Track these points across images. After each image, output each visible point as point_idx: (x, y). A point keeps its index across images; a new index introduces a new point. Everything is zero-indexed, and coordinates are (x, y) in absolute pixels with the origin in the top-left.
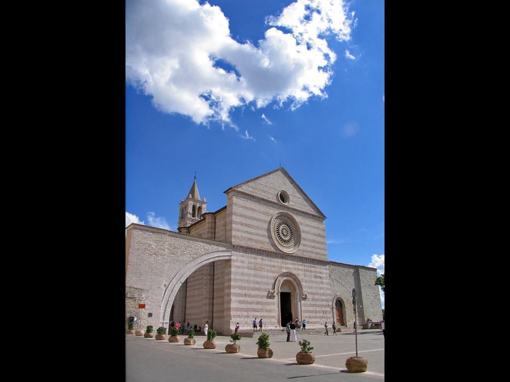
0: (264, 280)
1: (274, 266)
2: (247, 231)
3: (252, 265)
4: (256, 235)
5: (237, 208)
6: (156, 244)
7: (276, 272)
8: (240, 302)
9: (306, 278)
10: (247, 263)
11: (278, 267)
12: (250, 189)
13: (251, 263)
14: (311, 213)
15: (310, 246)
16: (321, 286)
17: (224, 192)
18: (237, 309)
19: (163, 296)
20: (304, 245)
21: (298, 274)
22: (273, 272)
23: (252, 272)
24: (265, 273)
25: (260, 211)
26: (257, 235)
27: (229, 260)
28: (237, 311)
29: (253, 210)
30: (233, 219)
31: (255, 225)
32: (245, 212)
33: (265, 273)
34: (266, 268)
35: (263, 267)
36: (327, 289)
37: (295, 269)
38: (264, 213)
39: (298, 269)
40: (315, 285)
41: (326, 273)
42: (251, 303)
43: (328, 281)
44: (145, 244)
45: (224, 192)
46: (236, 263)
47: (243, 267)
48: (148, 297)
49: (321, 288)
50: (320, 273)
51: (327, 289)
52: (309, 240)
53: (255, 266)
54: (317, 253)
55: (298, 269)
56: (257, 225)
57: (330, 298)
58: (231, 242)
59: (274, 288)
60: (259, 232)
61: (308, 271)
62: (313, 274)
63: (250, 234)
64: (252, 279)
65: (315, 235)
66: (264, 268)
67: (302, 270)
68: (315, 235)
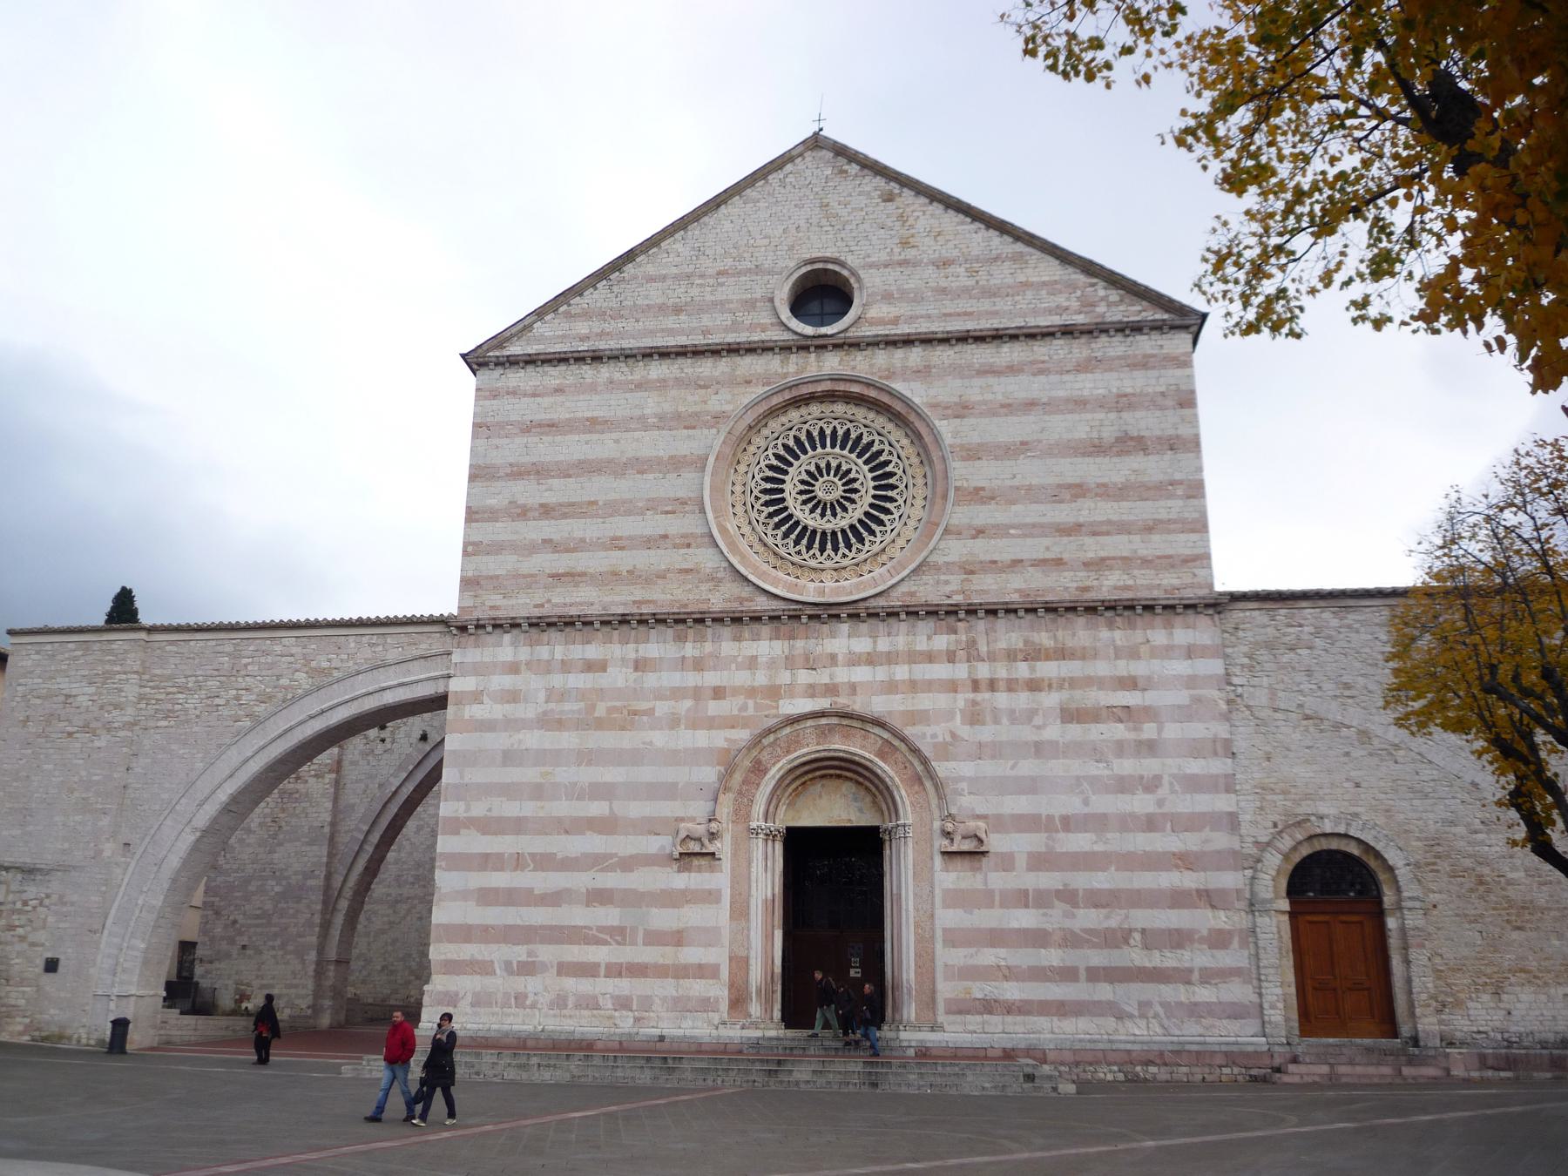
1: (718, 693)
2: (544, 541)
9: (986, 733)
11: (752, 692)
12: (582, 328)
14: (1057, 320)
20: (979, 532)
21: (916, 717)
22: (712, 724)
25: (642, 418)
26: (616, 544)
29: (594, 425)
31: (601, 499)
32: (545, 449)
37: (891, 687)
38: (667, 422)
39: (914, 686)
40: (1057, 767)
55: (914, 686)
56: (613, 496)
57: (1221, 841)
61: (1011, 686)
63: (574, 550)
67: (952, 687)
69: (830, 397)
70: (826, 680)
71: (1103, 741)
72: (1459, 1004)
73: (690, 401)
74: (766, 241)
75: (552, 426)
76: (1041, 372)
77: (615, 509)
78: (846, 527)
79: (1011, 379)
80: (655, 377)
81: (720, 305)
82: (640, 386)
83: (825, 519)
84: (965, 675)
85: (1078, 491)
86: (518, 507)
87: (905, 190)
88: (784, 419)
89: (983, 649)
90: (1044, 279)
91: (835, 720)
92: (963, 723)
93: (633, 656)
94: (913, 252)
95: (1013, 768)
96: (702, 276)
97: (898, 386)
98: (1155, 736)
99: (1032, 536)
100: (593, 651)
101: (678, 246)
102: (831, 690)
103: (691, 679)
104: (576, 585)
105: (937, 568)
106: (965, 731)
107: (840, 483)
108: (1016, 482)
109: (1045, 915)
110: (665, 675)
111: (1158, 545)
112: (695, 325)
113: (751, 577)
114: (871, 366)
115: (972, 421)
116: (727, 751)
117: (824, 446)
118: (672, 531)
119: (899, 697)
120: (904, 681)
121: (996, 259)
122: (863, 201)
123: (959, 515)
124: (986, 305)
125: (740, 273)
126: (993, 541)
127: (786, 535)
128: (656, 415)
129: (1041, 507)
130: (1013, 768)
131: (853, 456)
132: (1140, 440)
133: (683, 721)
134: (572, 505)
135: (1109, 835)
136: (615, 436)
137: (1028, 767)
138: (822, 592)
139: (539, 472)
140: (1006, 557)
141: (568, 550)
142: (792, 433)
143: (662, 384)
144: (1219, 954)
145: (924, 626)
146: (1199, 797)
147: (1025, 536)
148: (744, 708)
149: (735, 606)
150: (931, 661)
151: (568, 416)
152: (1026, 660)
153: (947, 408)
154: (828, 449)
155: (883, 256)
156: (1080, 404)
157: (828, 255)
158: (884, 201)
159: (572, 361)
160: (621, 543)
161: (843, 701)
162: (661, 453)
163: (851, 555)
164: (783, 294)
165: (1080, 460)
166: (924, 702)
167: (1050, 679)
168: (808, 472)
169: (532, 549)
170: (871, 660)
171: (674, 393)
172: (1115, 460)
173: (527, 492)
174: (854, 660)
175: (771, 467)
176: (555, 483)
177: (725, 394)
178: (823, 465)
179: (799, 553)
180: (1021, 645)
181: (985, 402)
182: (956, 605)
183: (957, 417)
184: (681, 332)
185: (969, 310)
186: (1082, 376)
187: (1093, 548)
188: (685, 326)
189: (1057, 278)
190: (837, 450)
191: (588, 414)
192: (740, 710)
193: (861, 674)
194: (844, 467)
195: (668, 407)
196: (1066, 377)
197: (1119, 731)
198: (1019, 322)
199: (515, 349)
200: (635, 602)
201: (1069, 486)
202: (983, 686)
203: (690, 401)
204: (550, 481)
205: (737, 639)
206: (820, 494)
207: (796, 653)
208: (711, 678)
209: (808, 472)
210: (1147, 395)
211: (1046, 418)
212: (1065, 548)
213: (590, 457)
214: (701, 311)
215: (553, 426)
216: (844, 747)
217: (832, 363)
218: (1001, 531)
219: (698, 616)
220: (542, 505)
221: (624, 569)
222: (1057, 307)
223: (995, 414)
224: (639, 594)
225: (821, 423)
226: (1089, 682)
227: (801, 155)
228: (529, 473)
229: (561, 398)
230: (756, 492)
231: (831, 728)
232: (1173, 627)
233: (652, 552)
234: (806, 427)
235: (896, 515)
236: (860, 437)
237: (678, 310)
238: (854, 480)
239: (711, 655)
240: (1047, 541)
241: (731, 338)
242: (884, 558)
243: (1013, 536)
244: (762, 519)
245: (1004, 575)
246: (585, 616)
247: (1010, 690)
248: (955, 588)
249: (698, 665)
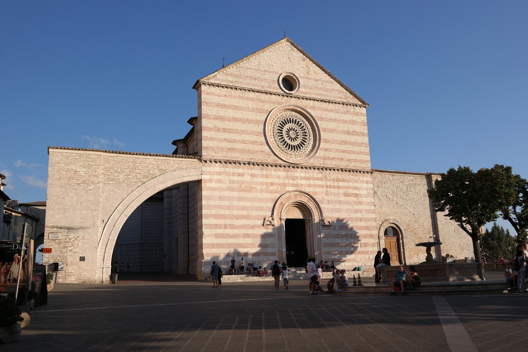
0: (256, 204)
1: (272, 184)
3: (236, 185)
4: (242, 143)
5: (209, 107)
6: (85, 170)
7: (275, 192)
8: (217, 236)
10: (228, 182)
11: (279, 184)
12: (231, 79)
13: (234, 182)
15: (337, 151)
16: (356, 207)
17: (194, 88)
18: (213, 246)
19: (99, 235)
20: (326, 150)
21: (315, 193)
22: (271, 192)
23: (235, 194)
24: (258, 195)
25: (248, 107)
26: (244, 142)
27: (199, 182)
28: (213, 248)
29: (235, 108)
30: (203, 125)
31: (239, 129)
32: (223, 112)
33: (258, 195)
34: (259, 187)
35: (254, 186)
36: (369, 211)
37: (309, 186)
39: (315, 186)
40: (344, 207)
41: (367, 189)
42: (235, 236)
43: (370, 199)
44: (68, 170)
45: (194, 88)
46: (209, 185)
47: (220, 189)
48: (78, 237)
49: (356, 211)
50: (356, 188)
51: (369, 211)
52: (335, 142)
53: (241, 186)
54: (350, 160)
55: (315, 186)
56: (242, 129)
57: (374, 224)
58: (201, 156)
59: (273, 214)
60: (247, 137)
61: (334, 187)
62: (342, 191)
63: (233, 142)
64: (235, 203)
65: (348, 133)
66: (256, 188)
67: (322, 186)
68: (348, 133)
69: (293, 110)
70: (296, 183)
71: (352, 201)
72: (412, 257)
74: (276, 64)
75: (224, 106)
76: (337, 112)
77: (243, 132)
78: (297, 145)
79: (331, 113)
80: (251, 97)
81: (266, 80)
82: (247, 99)
83: (292, 142)
84: (325, 184)
85: (345, 143)
86: (217, 128)
87: (307, 58)
88: (281, 114)
89: (328, 178)
90: (338, 89)
91: (298, 193)
92: (325, 195)
93: (251, 173)
94: (310, 76)
95: (335, 206)
96: (261, 71)
97: (308, 110)
98: (361, 201)
99: (337, 152)
100: (240, 170)
101: (254, 60)
102: (297, 185)
103: (265, 180)
104: (234, 152)
105: (318, 157)
106: (325, 197)
107: (295, 133)
108: (333, 139)
109: (342, 240)
110: (259, 178)
112: (260, 84)
113: (278, 155)
114: (302, 104)
115: (324, 122)
116: (275, 199)
117: (291, 123)
118: (258, 140)
119: (311, 188)
120: (312, 184)
121: (328, 81)
122: (297, 59)
124: (325, 93)
125: (270, 72)
126: (329, 152)
127: (283, 145)
128: (252, 108)
129: (338, 145)
130: (335, 206)
131: (297, 126)
132: (356, 132)
133: (264, 191)
134: (231, 129)
135: (354, 222)
136: (241, 112)
137: (338, 206)
138: (294, 161)
139: (222, 119)
140: (332, 156)
141: (231, 142)
142: (283, 118)
143: (252, 99)
144: (374, 248)
145: (316, 171)
146: (370, 215)
147: (335, 152)
148: (278, 188)
149: (274, 162)
150: (318, 180)
151: (228, 104)
152: (337, 181)
153: (319, 118)
154: (292, 124)
155: (304, 76)
156: (345, 122)
157: (291, 72)
158: (303, 60)
159: (229, 88)
160: (245, 142)
161: (300, 189)
162: (254, 119)
163: (298, 152)
165: (345, 135)
166: (317, 190)
167: (341, 186)
168: (287, 129)
169: (222, 140)
170: (305, 178)
171: (256, 102)
172: (352, 136)
173: (220, 124)
174: (302, 178)
175: (279, 126)
176: (226, 122)
177: (268, 105)
178: (291, 128)
179: (287, 150)
180: (336, 178)
181: (326, 118)
182: (324, 167)
183: (320, 120)
184: (256, 85)
185: (322, 94)
186: (345, 115)
187: (349, 156)
188: (257, 84)
189: (340, 89)
190: (294, 124)
191: (234, 104)
192: (277, 189)
193: (303, 182)
194: (296, 129)
195: (254, 106)
196: (343, 115)
197: (355, 199)
198: (332, 99)
200: (250, 158)
201: (344, 141)
202: (328, 187)
203: (260, 105)
204: (226, 122)
205: (275, 171)
206: (291, 135)
207: (289, 175)
208: (270, 180)
209: (287, 129)
210: (358, 122)
211: (339, 124)
212: (343, 155)
213: (236, 117)
214: (261, 81)
215: (225, 106)
216: (300, 200)
217: (293, 102)
219: (267, 164)
220: (223, 128)
221: (246, 149)
222: (340, 97)
223: (329, 121)
224: (251, 156)
225: (290, 117)
226: (348, 187)
227: (283, 42)
228: (219, 119)
229: (226, 98)
230: (276, 133)
231: (297, 195)
232: (364, 176)
233: (253, 145)
234: (286, 117)
235: (307, 143)
236: (298, 122)
237: (255, 79)
238: (298, 133)
239: (269, 174)
240: (340, 154)
241: (269, 90)
242: (305, 153)
243: (333, 152)
244: (277, 140)
245: (331, 161)
246: (239, 161)
247: (334, 188)
248: (321, 163)
249: (267, 176)
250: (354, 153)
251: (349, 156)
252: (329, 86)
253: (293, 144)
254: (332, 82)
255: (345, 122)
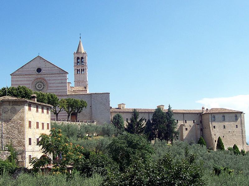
12: (20, 72)
29: (21, 81)
38: (27, 81)
52: (55, 87)
65: (60, 83)
69: (40, 79)
73: (28, 79)
75: (18, 81)
81: (31, 71)
85: (58, 87)
97: (45, 78)
111: (63, 91)
123: (49, 88)
124: (52, 71)
143: (27, 78)
156: (58, 80)
164: (36, 70)
187: (59, 91)
195: (27, 80)
199: (14, 74)
203: (28, 79)
212: (57, 91)
218: (52, 90)
237: (28, 71)
250: (61, 89)
251: (59, 91)
252: (53, 69)
253: (40, 89)
254: (54, 67)
255: (58, 80)
